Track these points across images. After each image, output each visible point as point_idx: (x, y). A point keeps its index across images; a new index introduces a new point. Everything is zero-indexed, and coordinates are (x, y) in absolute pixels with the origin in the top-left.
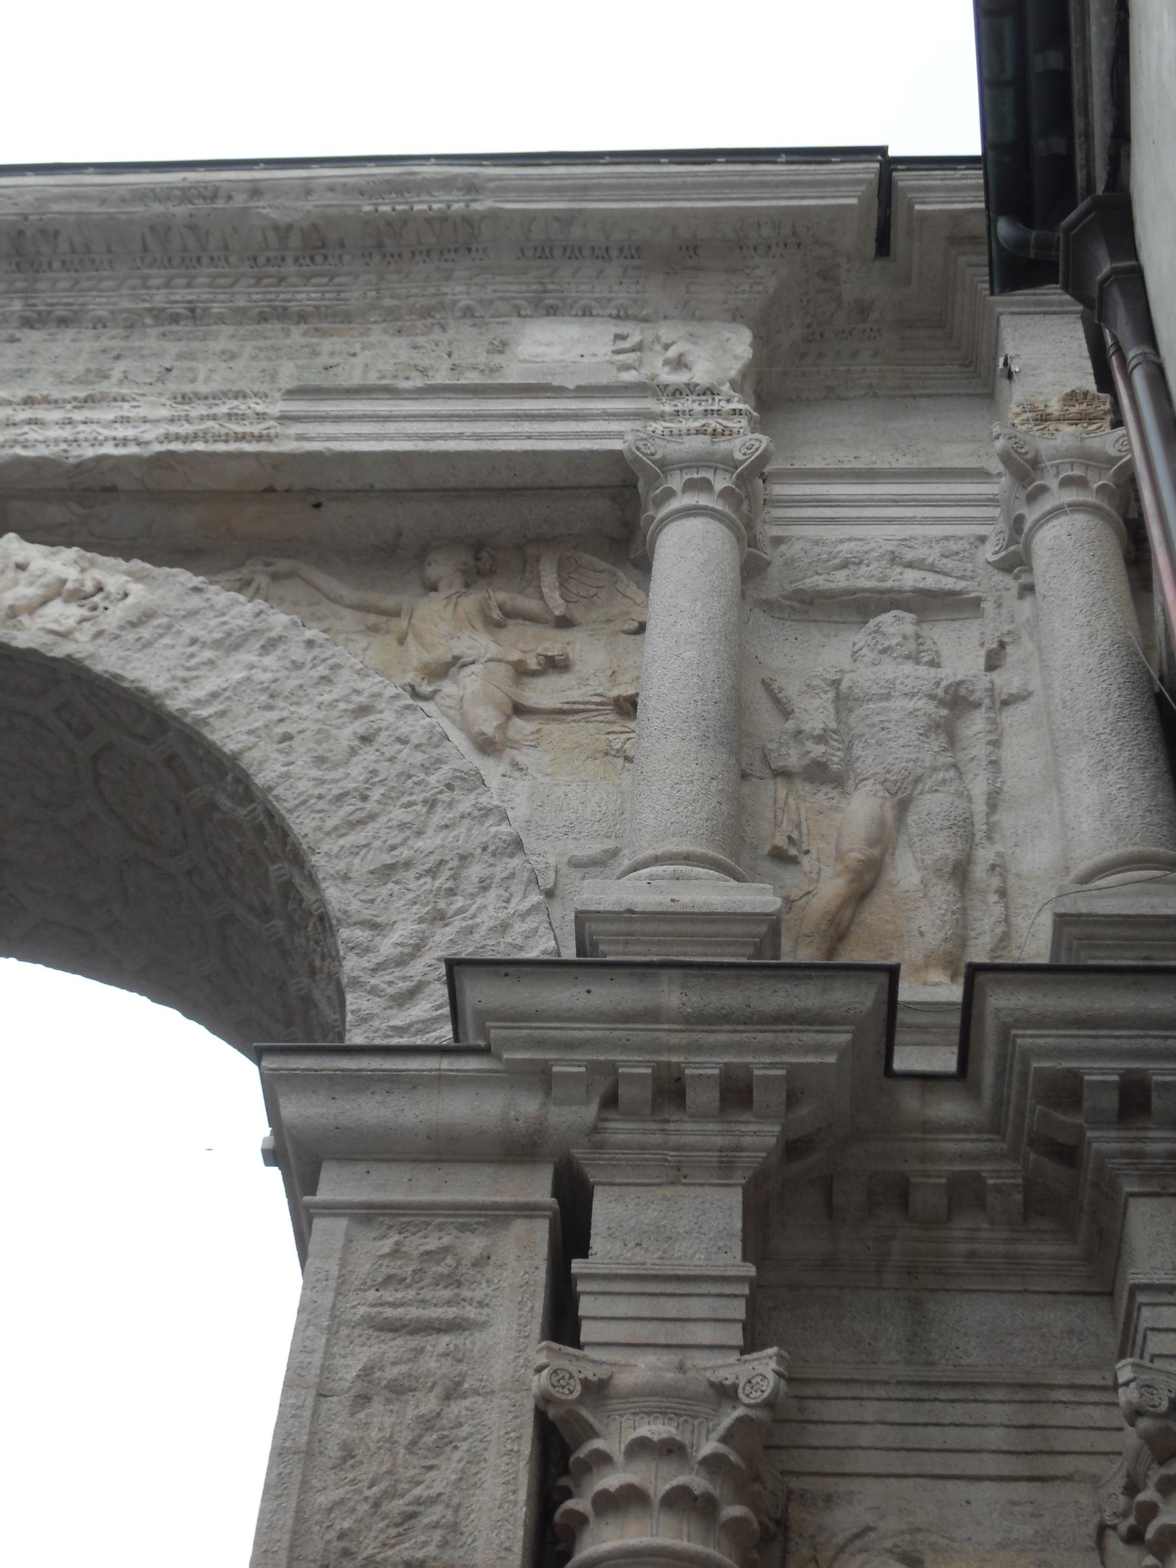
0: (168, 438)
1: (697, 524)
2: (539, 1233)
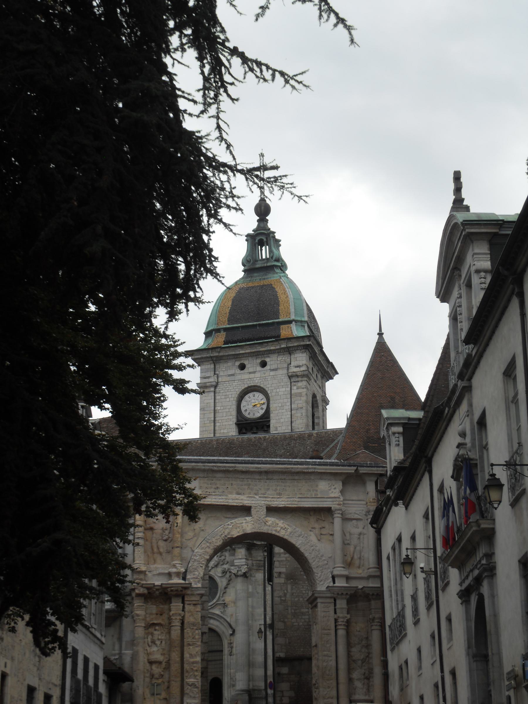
0: (287, 504)
1: (338, 518)
2: (333, 604)
